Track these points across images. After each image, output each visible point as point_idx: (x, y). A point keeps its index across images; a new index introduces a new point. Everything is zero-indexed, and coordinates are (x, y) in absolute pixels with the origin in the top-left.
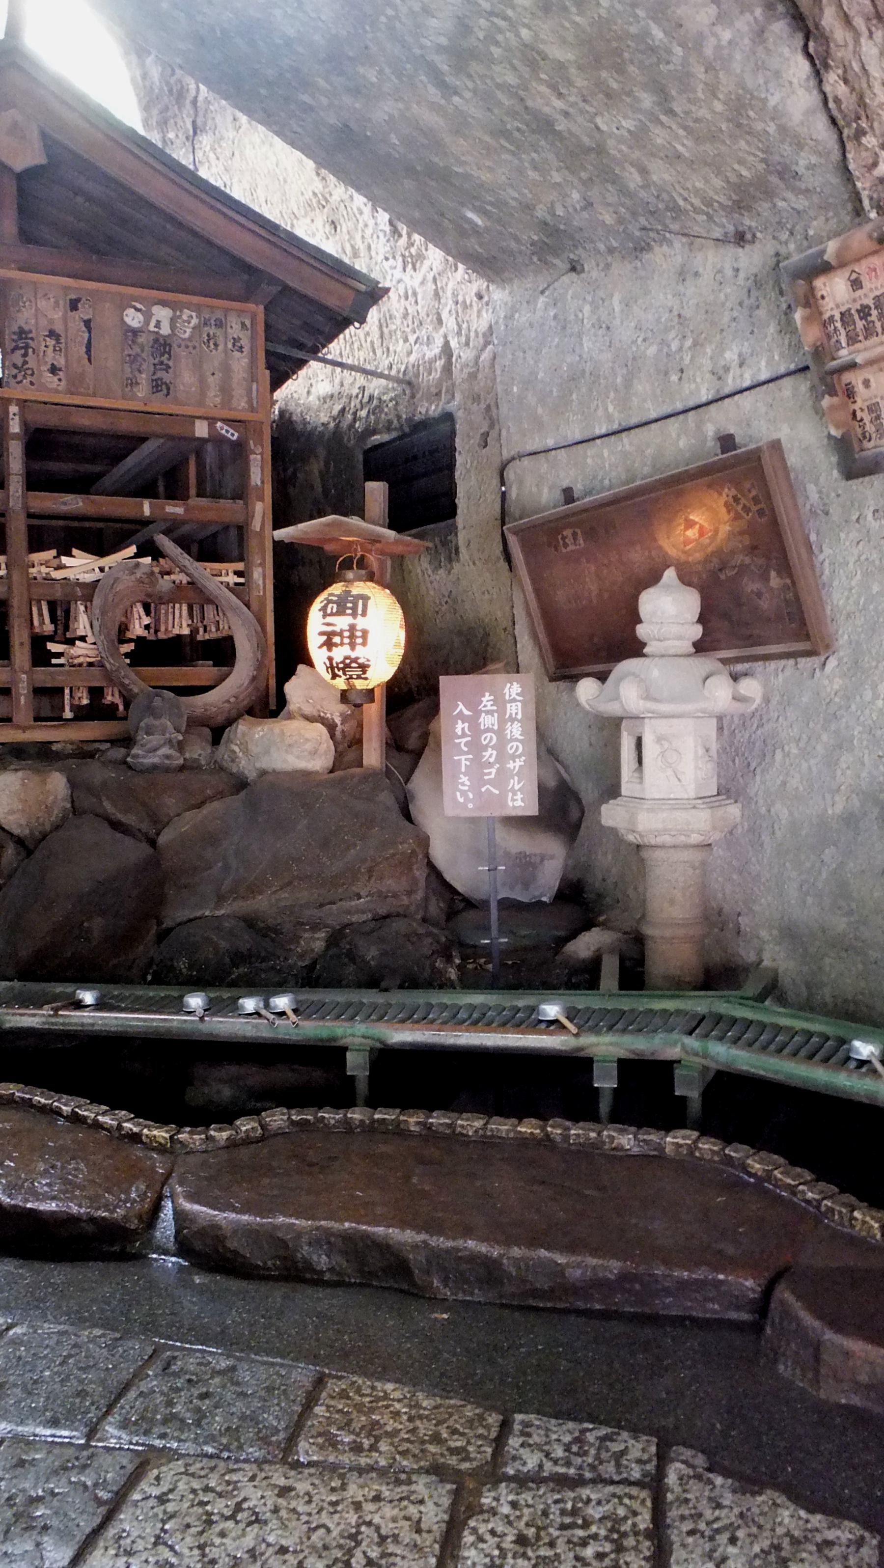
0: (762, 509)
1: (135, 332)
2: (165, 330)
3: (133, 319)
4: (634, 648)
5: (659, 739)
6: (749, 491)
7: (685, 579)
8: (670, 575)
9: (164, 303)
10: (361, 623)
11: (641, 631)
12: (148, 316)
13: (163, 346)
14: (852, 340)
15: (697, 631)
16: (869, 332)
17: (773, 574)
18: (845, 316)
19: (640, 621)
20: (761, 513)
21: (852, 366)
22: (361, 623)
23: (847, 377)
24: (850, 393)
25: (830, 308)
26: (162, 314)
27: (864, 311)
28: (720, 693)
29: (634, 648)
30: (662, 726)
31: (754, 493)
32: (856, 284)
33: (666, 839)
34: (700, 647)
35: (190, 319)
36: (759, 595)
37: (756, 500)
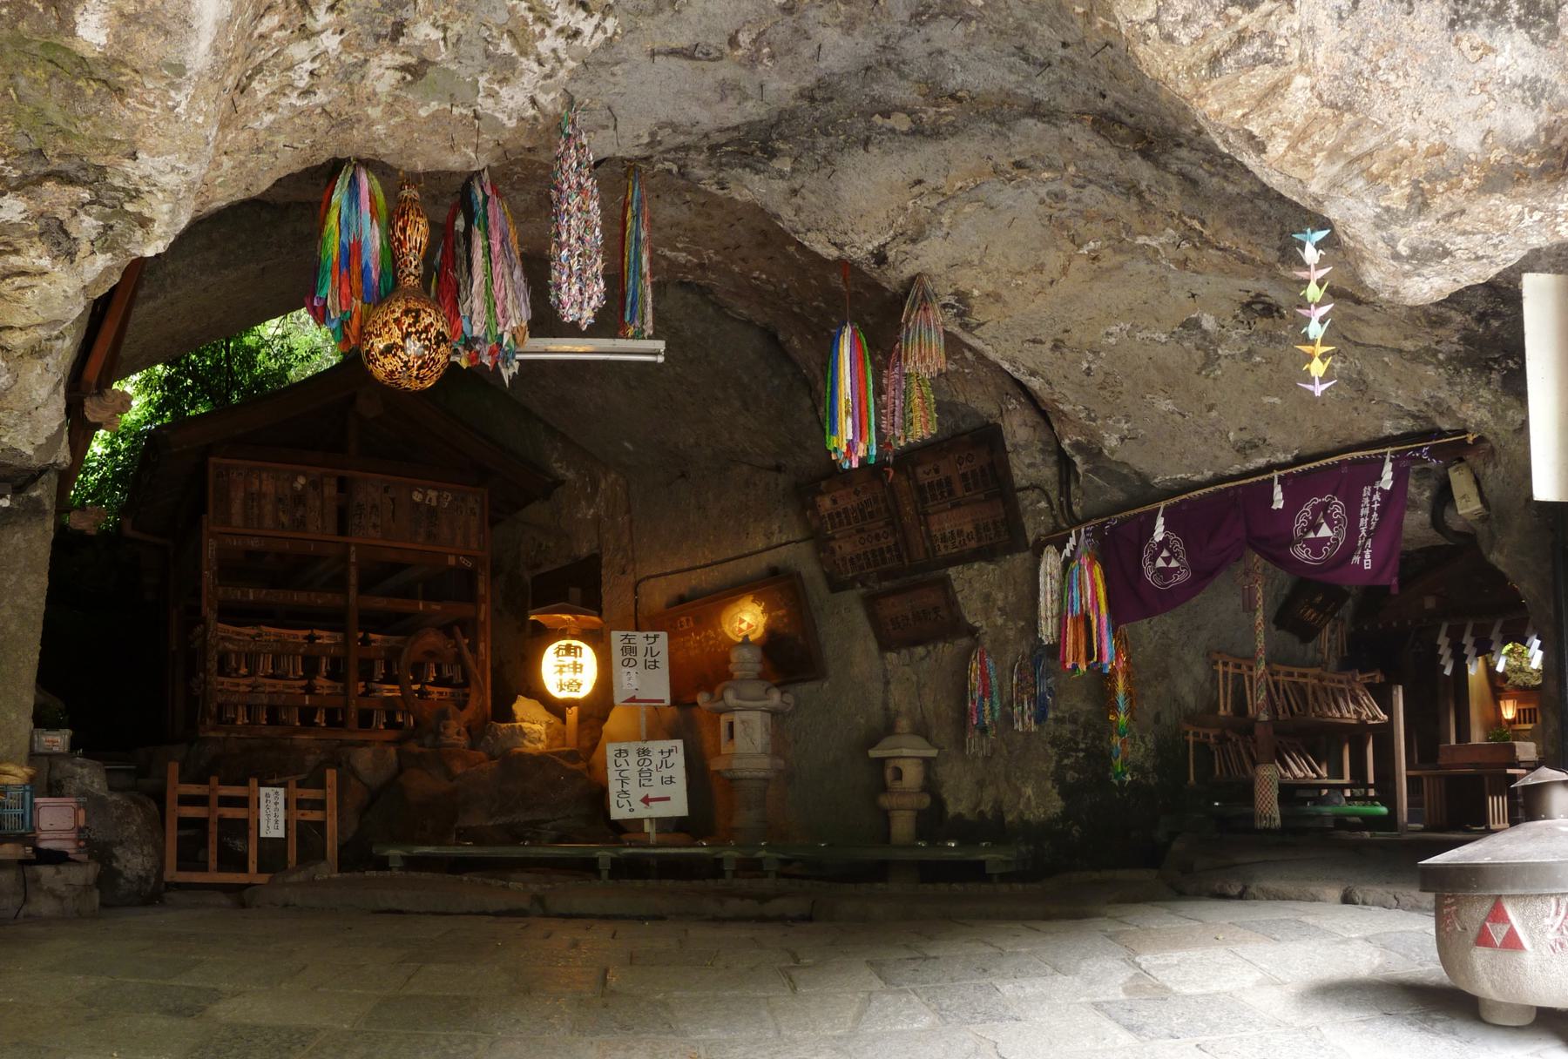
1: (418, 504)
2: (434, 503)
3: (417, 497)
4: (729, 676)
5: (743, 722)
9: (434, 489)
10: (579, 660)
11: (731, 667)
12: (425, 495)
13: (432, 512)
14: (833, 527)
15: (759, 668)
16: (841, 523)
18: (830, 515)
21: (833, 538)
22: (579, 660)
23: (832, 544)
24: (833, 551)
25: (823, 512)
26: (432, 494)
27: (838, 514)
28: (775, 698)
30: (744, 715)
32: (834, 501)
34: (762, 677)
35: (448, 497)
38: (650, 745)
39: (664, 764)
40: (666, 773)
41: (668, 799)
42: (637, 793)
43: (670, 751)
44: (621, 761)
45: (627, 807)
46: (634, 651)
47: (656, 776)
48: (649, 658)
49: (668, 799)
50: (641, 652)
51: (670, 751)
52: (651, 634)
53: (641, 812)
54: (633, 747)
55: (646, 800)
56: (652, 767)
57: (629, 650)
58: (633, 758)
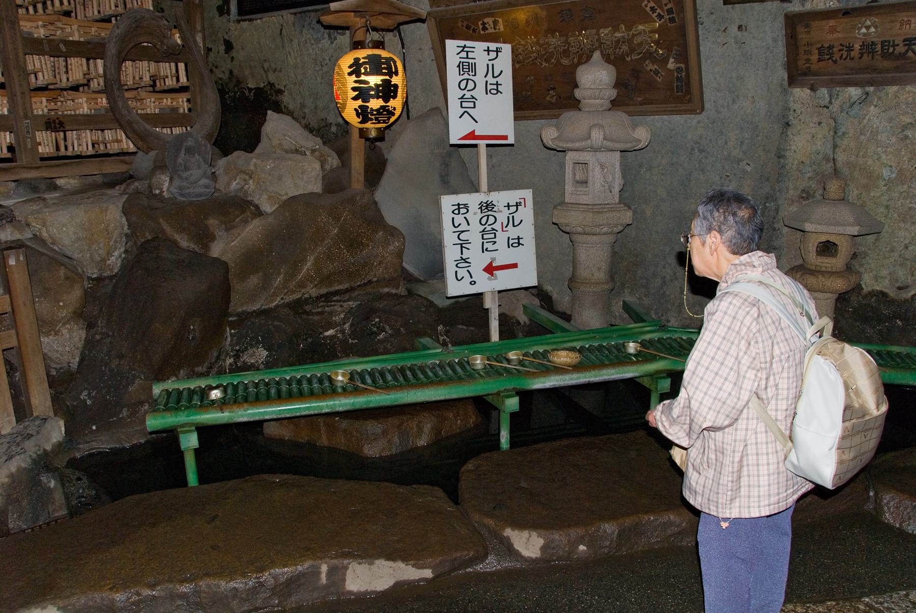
0: (673, 18)
4: (574, 104)
6: (666, 5)
7: (607, 59)
8: (597, 55)
15: (613, 93)
17: (672, 60)
19: (576, 86)
20: (672, 20)
29: (574, 104)
31: (669, 6)
33: (580, 229)
34: (615, 104)
36: (656, 73)
37: (670, 11)
38: (494, 197)
39: (512, 221)
40: (513, 232)
41: (515, 266)
42: (479, 261)
43: (517, 205)
44: (459, 219)
45: (467, 279)
46: (472, 68)
47: (502, 238)
48: (490, 79)
49: (515, 266)
50: (481, 69)
51: (517, 205)
52: (493, 46)
53: (485, 285)
54: (473, 200)
55: (490, 269)
56: (497, 226)
57: (468, 67)
58: (474, 215)
